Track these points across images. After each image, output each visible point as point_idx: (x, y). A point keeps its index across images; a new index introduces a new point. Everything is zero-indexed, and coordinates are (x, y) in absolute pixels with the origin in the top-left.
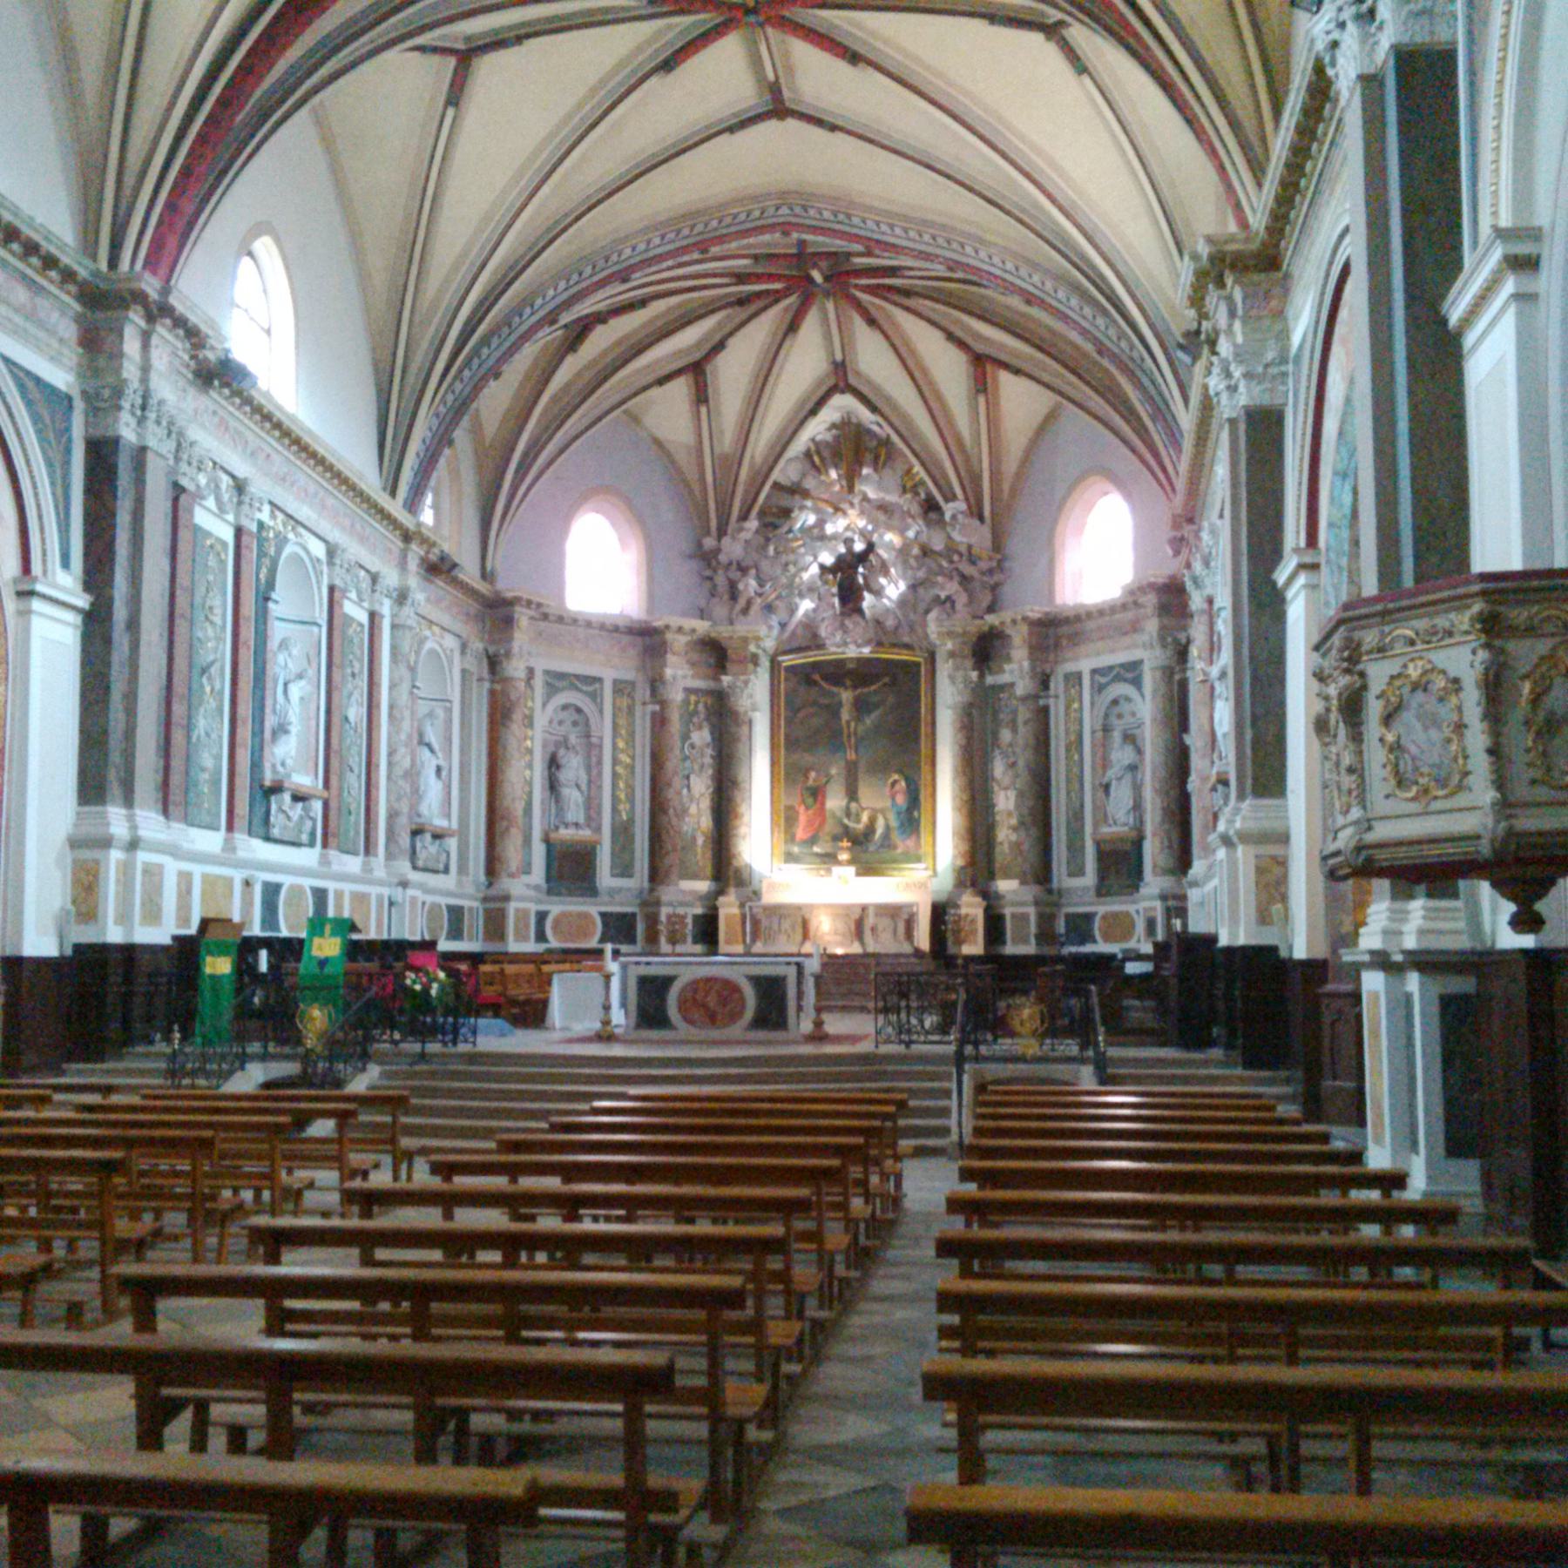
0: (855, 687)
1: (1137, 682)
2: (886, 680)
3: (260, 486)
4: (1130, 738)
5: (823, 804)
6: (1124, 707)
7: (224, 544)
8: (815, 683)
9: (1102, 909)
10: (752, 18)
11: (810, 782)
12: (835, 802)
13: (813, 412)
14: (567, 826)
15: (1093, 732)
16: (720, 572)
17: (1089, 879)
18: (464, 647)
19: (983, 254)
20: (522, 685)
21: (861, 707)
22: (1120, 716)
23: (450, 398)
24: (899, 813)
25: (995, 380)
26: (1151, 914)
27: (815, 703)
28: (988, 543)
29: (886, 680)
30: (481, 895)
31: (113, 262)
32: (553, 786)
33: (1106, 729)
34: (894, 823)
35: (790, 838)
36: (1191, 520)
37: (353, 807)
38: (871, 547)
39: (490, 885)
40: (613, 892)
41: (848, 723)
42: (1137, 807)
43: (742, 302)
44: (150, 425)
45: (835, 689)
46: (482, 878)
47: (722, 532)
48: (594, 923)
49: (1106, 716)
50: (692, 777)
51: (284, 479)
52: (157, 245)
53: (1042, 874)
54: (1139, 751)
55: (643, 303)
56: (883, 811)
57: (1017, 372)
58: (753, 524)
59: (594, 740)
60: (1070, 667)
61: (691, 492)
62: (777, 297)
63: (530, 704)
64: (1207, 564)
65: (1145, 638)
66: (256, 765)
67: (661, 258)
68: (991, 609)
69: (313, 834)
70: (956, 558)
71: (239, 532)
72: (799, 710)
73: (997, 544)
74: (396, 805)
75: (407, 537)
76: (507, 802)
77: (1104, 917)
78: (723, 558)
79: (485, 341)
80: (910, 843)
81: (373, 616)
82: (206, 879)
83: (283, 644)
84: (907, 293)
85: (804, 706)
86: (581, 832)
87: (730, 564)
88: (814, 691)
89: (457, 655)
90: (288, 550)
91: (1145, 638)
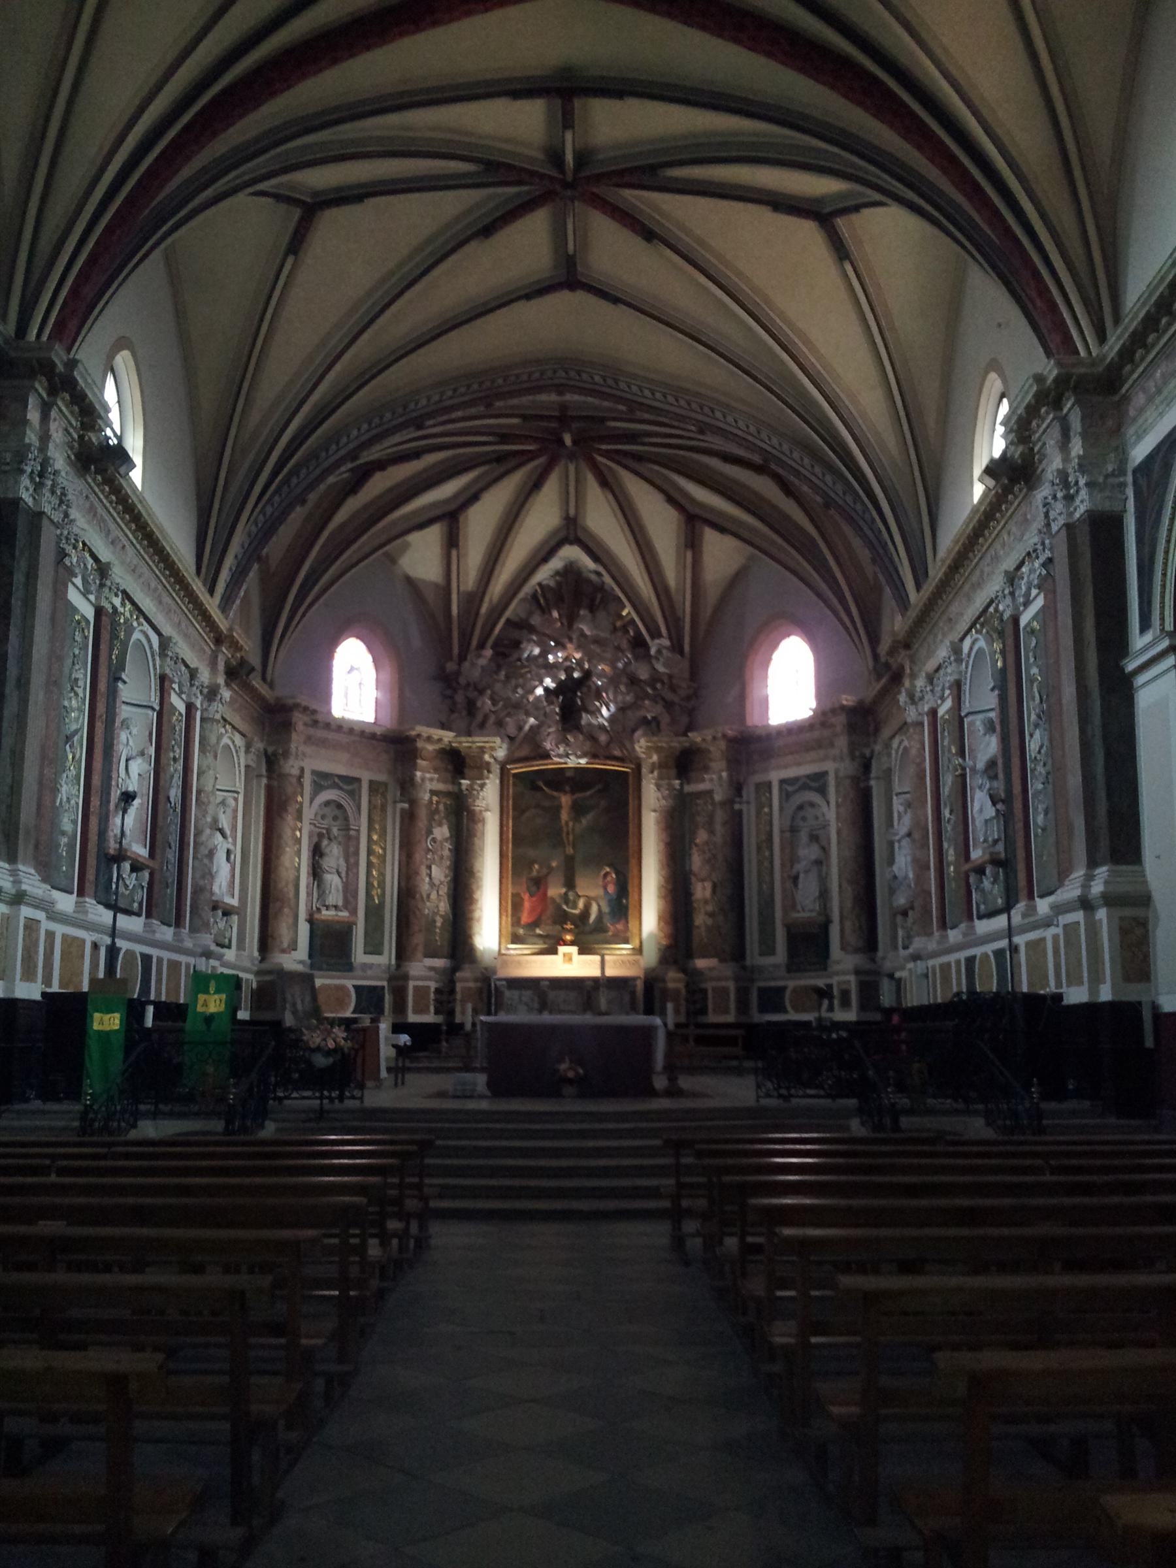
0: (573, 792)
1: (822, 791)
2: (599, 786)
3: (120, 575)
4: (814, 838)
5: (545, 894)
6: (809, 812)
7: (88, 622)
8: (539, 789)
9: (791, 984)
10: (569, 193)
11: (535, 873)
12: (555, 891)
13: (545, 559)
14: (327, 908)
15: (782, 832)
16: (461, 692)
17: (780, 956)
18: (248, 747)
19: (730, 419)
20: (294, 781)
21: (578, 810)
22: (804, 819)
23: (261, 518)
24: (610, 901)
25: (701, 535)
26: (844, 987)
27: (538, 806)
28: (686, 675)
29: (599, 786)
30: (255, 968)
31: (22, 330)
32: (316, 872)
33: (794, 830)
34: (606, 909)
35: (516, 922)
36: (907, 646)
37: (170, 880)
38: (587, 675)
39: (263, 960)
40: (365, 967)
41: (567, 823)
42: (824, 894)
43: (500, 458)
44: (46, 491)
45: (555, 794)
46: (256, 954)
47: (462, 658)
48: (349, 996)
49: (793, 819)
50: (433, 867)
51: (134, 571)
52: (60, 325)
53: (738, 954)
54: (825, 850)
55: (416, 454)
56: (595, 899)
57: (722, 530)
58: (488, 652)
59: (352, 833)
60: (758, 778)
62: (530, 456)
63: (299, 799)
64: (930, 679)
65: (835, 752)
66: (102, 833)
67: (452, 408)
68: (690, 728)
69: (141, 904)
70: (659, 686)
71: (99, 611)
72: (523, 812)
73: (694, 673)
74: (201, 883)
75: (219, 640)
76: (281, 885)
77: (794, 990)
78: (462, 681)
79: (294, 472)
80: (620, 926)
81: (190, 707)
82: (65, 937)
83: (125, 724)
84: (639, 458)
86: (340, 914)
87: (468, 685)
89: (243, 749)
90: (137, 635)
91: (835, 752)
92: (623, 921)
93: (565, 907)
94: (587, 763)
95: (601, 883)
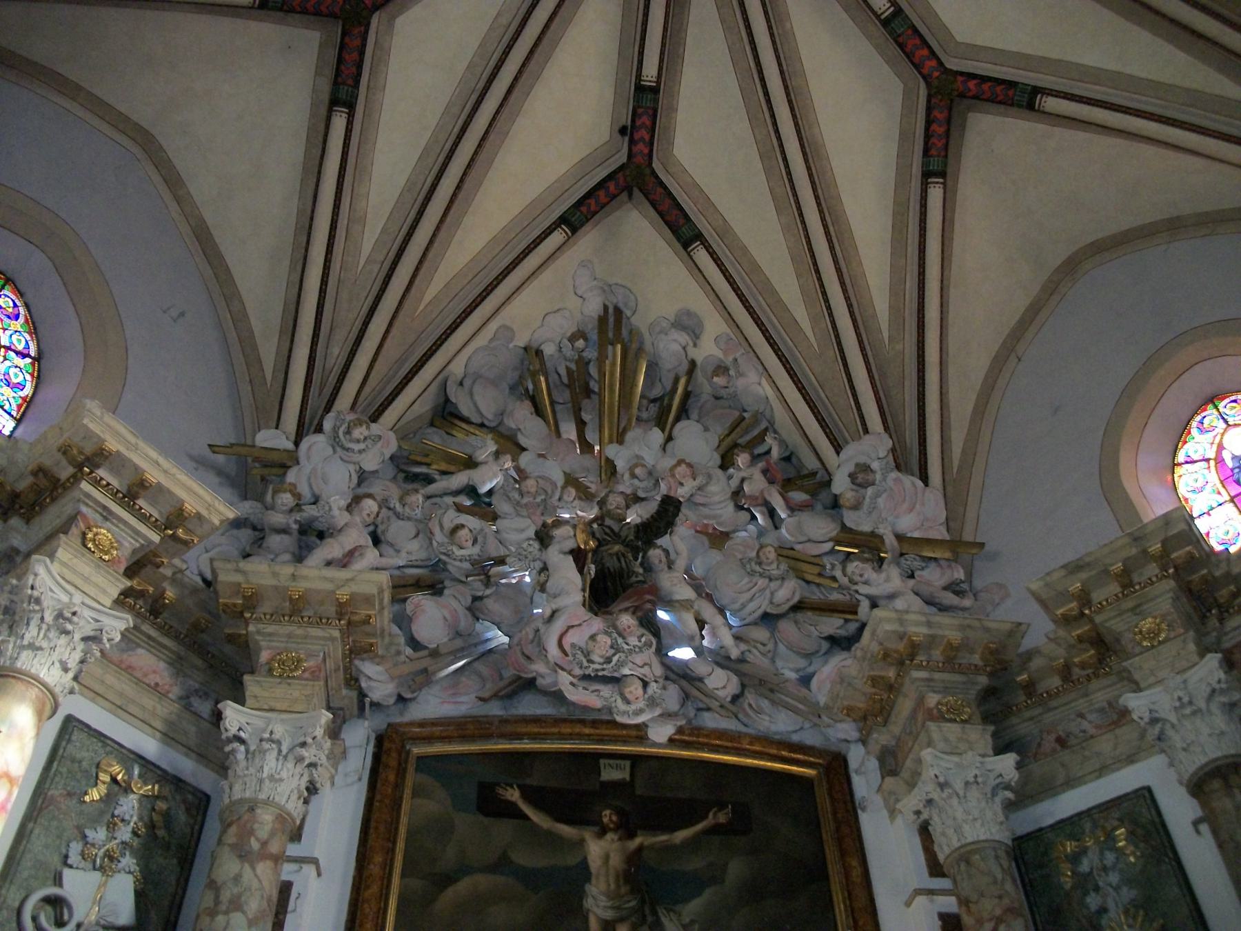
0: (627, 830)
8: (512, 812)
27: (501, 864)
45: (565, 830)
61: (248, 343)
72: (446, 880)
85: (464, 870)
88: (503, 830)
94: (671, 741)
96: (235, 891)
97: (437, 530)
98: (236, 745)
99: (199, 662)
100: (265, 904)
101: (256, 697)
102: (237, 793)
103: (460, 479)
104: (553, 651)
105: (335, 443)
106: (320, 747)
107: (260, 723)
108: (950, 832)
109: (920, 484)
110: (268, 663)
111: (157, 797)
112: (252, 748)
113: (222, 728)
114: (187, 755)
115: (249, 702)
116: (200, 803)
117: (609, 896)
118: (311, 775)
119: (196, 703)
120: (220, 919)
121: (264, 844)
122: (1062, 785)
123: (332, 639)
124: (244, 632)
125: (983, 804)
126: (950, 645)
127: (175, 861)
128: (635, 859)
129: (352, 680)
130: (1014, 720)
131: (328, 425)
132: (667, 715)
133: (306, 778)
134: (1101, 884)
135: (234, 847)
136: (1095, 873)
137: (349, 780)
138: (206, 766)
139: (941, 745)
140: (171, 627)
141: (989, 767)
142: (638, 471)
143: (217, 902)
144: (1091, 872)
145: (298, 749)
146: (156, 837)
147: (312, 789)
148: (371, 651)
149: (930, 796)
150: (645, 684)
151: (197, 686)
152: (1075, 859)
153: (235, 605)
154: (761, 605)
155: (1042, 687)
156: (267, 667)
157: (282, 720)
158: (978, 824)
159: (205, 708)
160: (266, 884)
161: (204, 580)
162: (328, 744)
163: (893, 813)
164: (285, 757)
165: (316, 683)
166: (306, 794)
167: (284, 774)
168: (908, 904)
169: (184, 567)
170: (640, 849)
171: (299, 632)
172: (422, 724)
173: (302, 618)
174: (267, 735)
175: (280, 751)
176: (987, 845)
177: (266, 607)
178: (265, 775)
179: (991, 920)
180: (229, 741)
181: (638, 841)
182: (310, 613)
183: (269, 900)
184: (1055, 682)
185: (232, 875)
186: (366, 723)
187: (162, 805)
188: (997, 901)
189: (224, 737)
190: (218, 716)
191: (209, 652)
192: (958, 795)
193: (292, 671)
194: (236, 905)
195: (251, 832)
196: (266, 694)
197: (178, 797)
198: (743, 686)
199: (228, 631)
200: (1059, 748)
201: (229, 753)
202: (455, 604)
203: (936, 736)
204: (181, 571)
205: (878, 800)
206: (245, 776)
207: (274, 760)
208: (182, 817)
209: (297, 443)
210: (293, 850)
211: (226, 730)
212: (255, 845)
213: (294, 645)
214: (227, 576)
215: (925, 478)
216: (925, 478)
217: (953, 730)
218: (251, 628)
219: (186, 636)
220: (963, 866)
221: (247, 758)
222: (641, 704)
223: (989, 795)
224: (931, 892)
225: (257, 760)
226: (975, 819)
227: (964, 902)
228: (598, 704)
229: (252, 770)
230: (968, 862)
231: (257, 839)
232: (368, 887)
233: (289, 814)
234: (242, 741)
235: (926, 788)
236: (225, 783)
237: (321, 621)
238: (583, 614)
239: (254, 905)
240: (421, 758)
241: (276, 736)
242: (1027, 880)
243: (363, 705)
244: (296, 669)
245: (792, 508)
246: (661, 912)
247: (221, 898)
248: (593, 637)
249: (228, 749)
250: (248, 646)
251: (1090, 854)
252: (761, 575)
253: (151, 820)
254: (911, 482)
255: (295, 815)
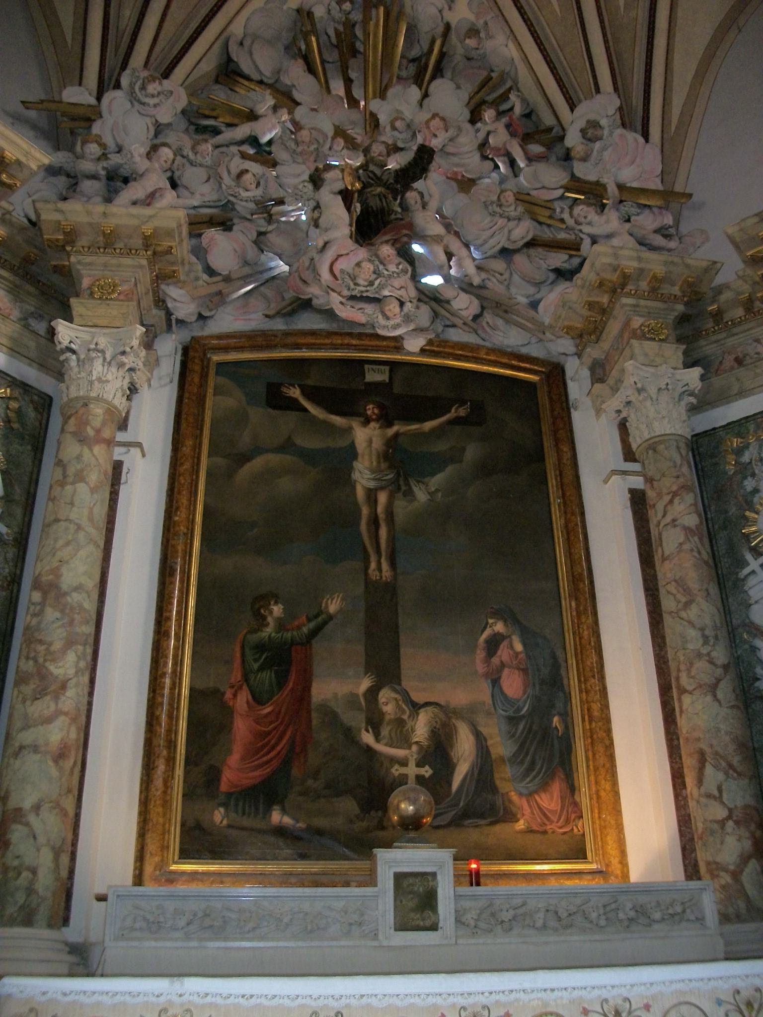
0: (386, 420)
5: (303, 695)
8: (293, 405)
11: (269, 631)
24: (513, 720)
27: (287, 446)
45: (337, 420)
56: (469, 714)
72: (244, 459)
80: (550, 800)
85: (258, 450)
88: (288, 421)
92: (557, 787)
93: (368, 738)
94: (423, 351)
95: (481, 668)
96: (79, 467)
97: (225, 175)
98: (68, 354)
99: (32, 289)
100: (102, 477)
101: (81, 316)
102: (73, 393)
103: (243, 131)
104: (325, 275)
105: (133, 98)
106: (138, 356)
107: (87, 337)
108: (643, 427)
109: (641, 140)
110: (89, 288)
111: (9, 398)
112: (82, 357)
113: (56, 342)
114: (30, 365)
115: (76, 320)
116: (45, 403)
117: (372, 471)
118: (132, 377)
119: (32, 322)
120: (69, 488)
121: (98, 431)
122: (736, 395)
123: (141, 267)
124: (67, 263)
125: (671, 406)
126: (655, 277)
127: (29, 447)
128: (392, 443)
129: (160, 302)
130: (702, 342)
131: (125, 81)
132: (420, 330)
133: (127, 380)
134: (757, 472)
135: (74, 434)
136: (753, 462)
137: (163, 382)
138: (47, 374)
139: (641, 358)
140: (6, 260)
141: (678, 377)
142: (398, 124)
143: (65, 476)
144: (750, 463)
145: (120, 357)
146: (12, 429)
147: (133, 389)
148: (174, 276)
149: (629, 399)
150: (402, 304)
151: (32, 309)
152: (739, 452)
153: (57, 240)
154: (500, 241)
155: (727, 317)
156: (89, 291)
157: (104, 334)
158: (666, 421)
159: (41, 327)
160: (101, 461)
161: (30, 221)
162: (143, 353)
163: (598, 412)
164: (110, 363)
165: (130, 303)
166: (128, 392)
167: (110, 377)
168: (606, 481)
169: (11, 208)
170: (397, 435)
171: (114, 261)
172: (220, 337)
173: (115, 249)
174: (93, 346)
175: (105, 359)
176: (671, 437)
177: (83, 241)
178: (94, 378)
179: (668, 494)
180: (63, 352)
181: (395, 428)
182: (121, 245)
183: (105, 474)
184: (739, 312)
185: (74, 456)
186: (174, 336)
187: (14, 405)
188: (674, 480)
189: (58, 348)
190: (52, 332)
191: (39, 281)
192: (651, 399)
193: (109, 294)
194: (80, 477)
195: (87, 423)
196: (90, 313)
197: (26, 398)
198: (483, 308)
199: (53, 263)
200: (736, 365)
201: (63, 361)
202: (242, 237)
203: (637, 351)
204: (9, 213)
205: (588, 401)
206: (79, 378)
207: (101, 366)
208: (31, 413)
209: (99, 98)
210: (121, 437)
211: (60, 343)
212: (90, 432)
213: (110, 273)
214: (49, 215)
215: (646, 135)
216: (646, 135)
217: (651, 347)
218: (73, 259)
219: (19, 268)
220: (650, 452)
221: (78, 365)
222: (398, 320)
223: (677, 400)
224: (624, 473)
225: (87, 366)
226: (664, 417)
227: (649, 480)
228: (363, 319)
229: (83, 374)
230: (655, 450)
231: (92, 428)
232: (182, 464)
233: (116, 408)
234: (74, 352)
235: (626, 392)
236: (63, 386)
237: (129, 252)
238: (351, 245)
239: (93, 477)
240: (220, 364)
241: (100, 347)
242: (700, 467)
243: (170, 322)
244: (113, 292)
245: (531, 159)
246: (412, 483)
247: (68, 473)
248: (358, 265)
249: (62, 358)
250: (71, 276)
251: (751, 448)
252: (501, 216)
253: (7, 416)
254: (634, 138)
255: (121, 408)
